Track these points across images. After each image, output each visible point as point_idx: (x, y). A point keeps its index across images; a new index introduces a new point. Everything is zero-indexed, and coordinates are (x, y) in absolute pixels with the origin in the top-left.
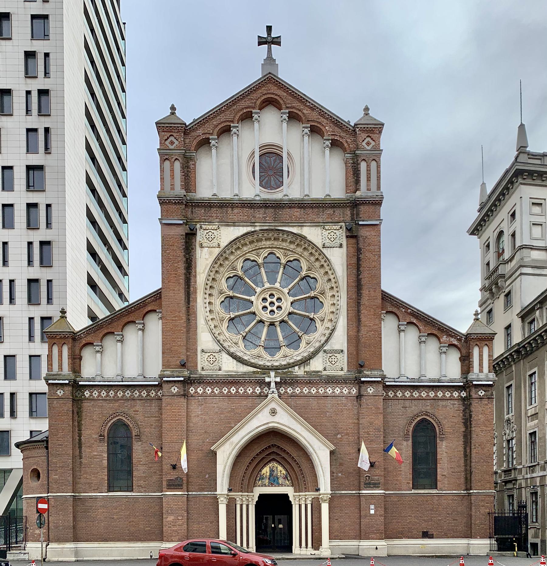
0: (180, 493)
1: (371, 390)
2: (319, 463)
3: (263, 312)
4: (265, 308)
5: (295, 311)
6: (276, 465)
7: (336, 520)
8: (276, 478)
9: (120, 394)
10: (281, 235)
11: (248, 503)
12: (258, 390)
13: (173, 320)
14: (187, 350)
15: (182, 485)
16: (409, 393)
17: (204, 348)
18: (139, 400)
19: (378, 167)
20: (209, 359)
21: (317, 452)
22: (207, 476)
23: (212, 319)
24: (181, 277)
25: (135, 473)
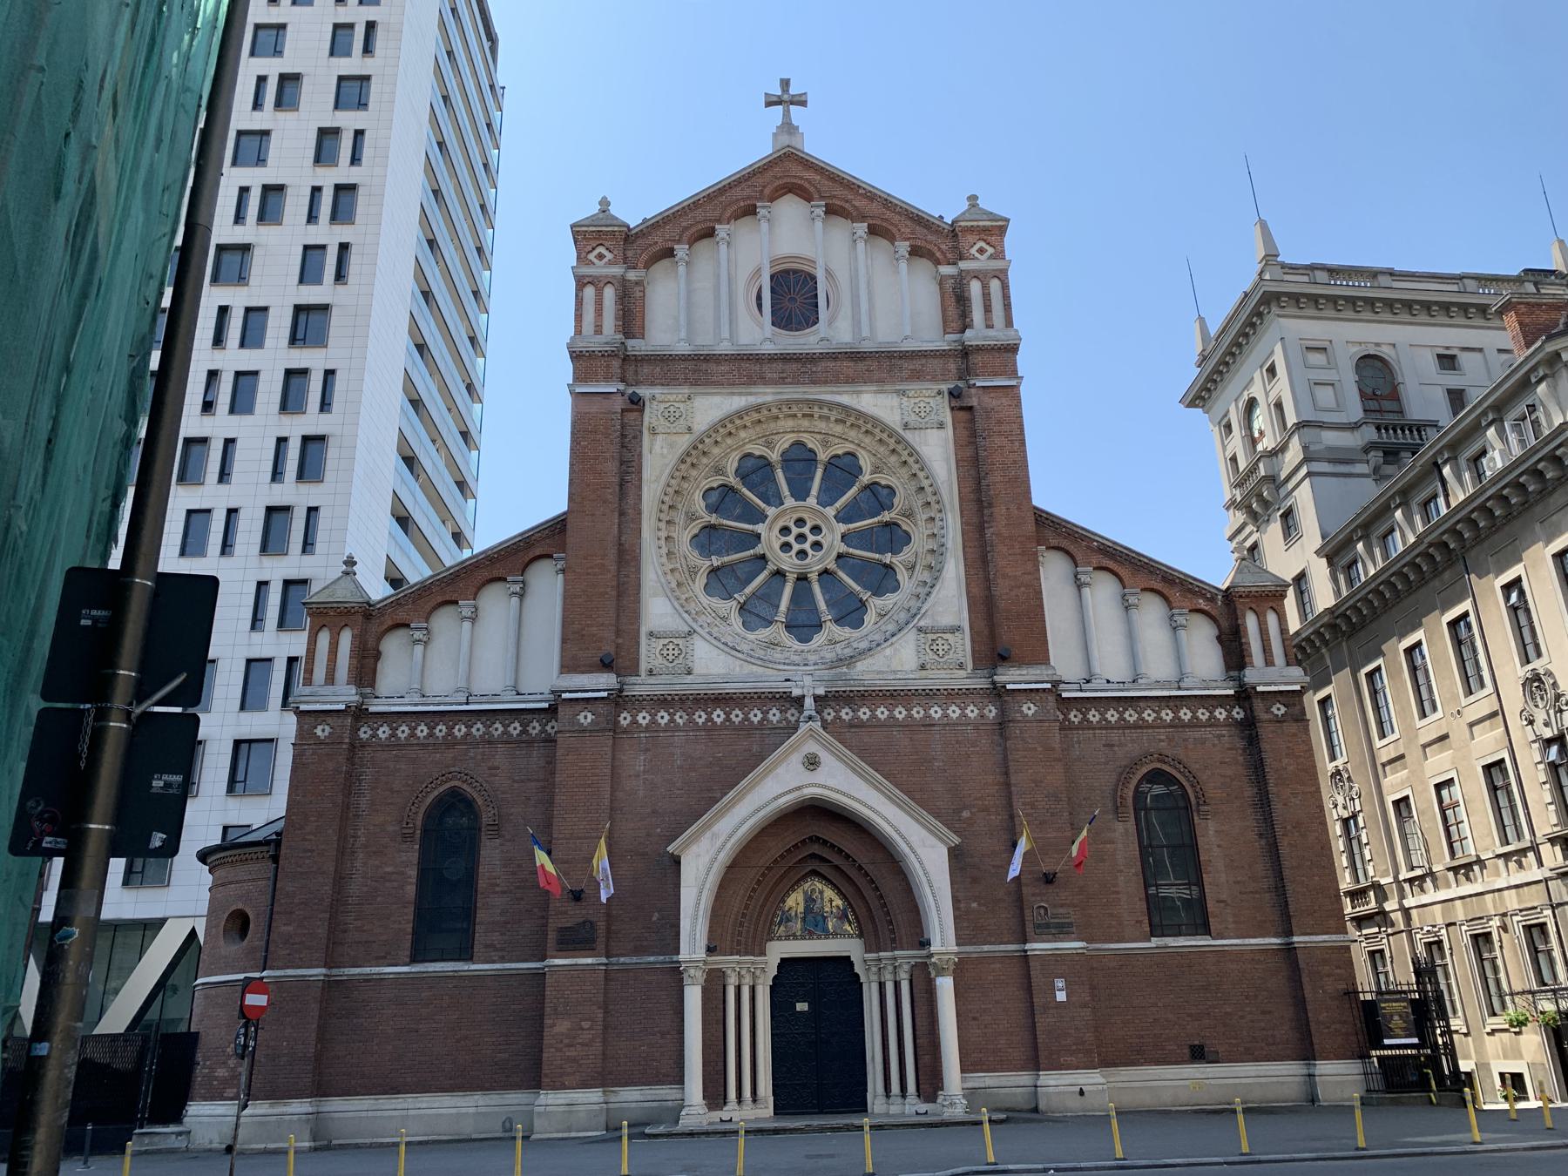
0: (589, 961)
1: (1029, 709)
2: (924, 879)
4: (786, 547)
6: (820, 886)
7: (974, 1019)
8: (819, 918)
9: (460, 730)
10: (816, 409)
11: (754, 981)
13: (588, 574)
14: (618, 633)
15: (594, 941)
16: (1115, 713)
17: (655, 629)
18: (502, 742)
19: (1005, 287)
20: (665, 652)
22: (656, 916)
23: (672, 571)
25: (481, 915)
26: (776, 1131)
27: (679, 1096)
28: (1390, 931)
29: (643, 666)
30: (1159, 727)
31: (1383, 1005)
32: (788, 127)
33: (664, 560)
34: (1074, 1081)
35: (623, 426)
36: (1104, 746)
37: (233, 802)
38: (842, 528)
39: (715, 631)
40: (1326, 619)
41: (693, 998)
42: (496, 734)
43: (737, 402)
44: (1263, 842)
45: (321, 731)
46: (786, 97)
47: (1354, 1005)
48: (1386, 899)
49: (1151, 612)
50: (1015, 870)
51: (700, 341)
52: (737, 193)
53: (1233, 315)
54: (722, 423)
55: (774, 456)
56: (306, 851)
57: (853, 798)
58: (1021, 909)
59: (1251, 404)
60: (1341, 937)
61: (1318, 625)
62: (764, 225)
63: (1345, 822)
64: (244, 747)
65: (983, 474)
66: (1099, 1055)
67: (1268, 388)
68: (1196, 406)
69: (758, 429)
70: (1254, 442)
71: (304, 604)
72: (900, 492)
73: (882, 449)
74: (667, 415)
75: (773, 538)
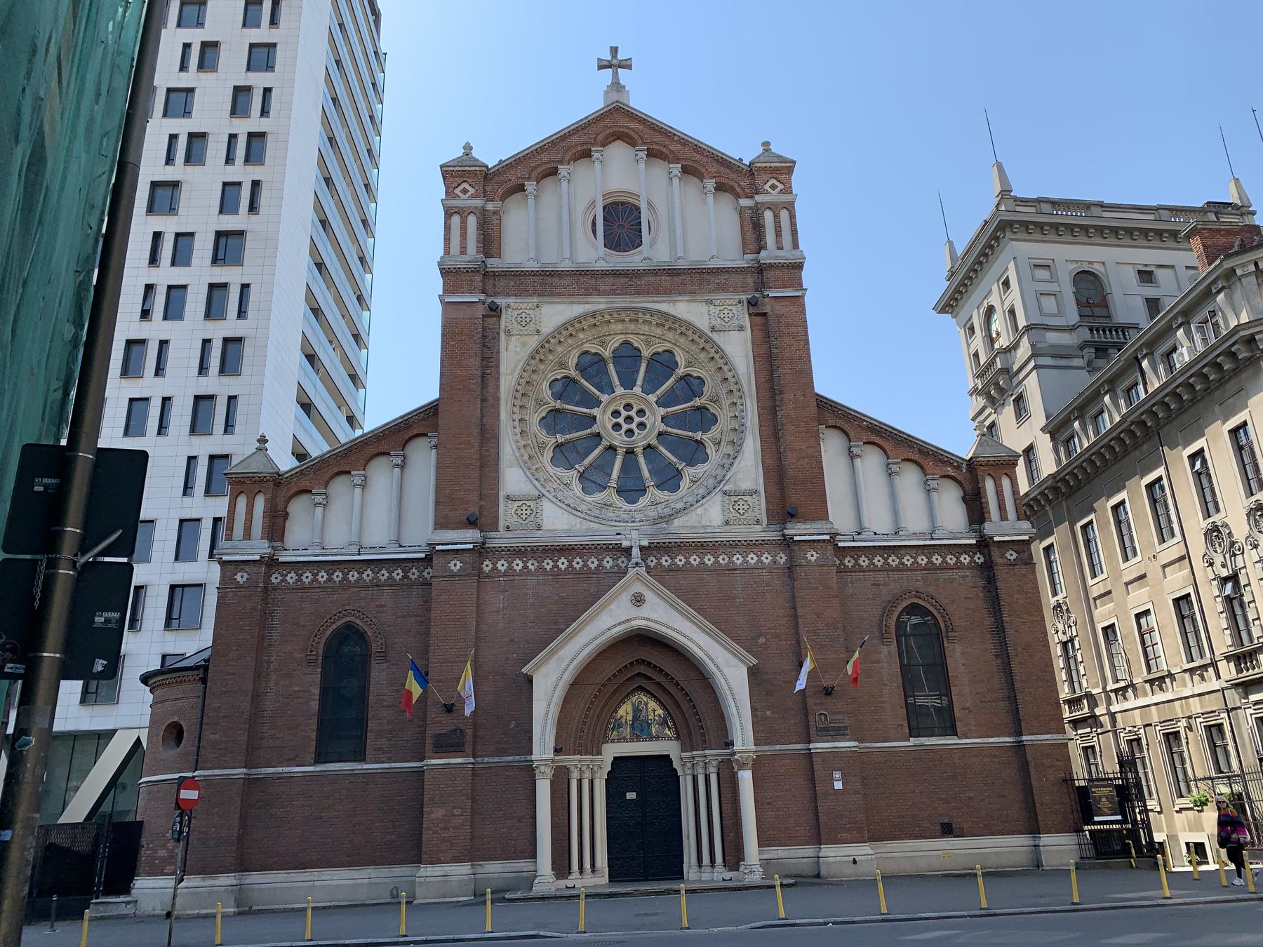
0: (460, 760)
1: (812, 556)
2: (728, 692)
3: (613, 432)
4: (617, 427)
5: (669, 429)
6: (645, 699)
7: (769, 804)
9: (353, 576)
10: (640, 315)
12: (608, 562)
13: (457, 449)
14: (481, 496)
15: (463, 745)
18: (387, 586)
19: (792, 217)
21: (724, 670)
24: (472, 382)
25: (371, 725)
26: (610, 895)
27: (532, 868)
28: (1099, 731)
29: (502, 524)
30: (916, 570)
31: (1093, 790)
32: (616, 86)
33: (518, 437)
34: (846, 853)
35: (484, 329)
36: (872, 585)
37: (169, 636)
38: (662, 411)
39: (560, 495)
40: (1049, 483)
41: (543, 790)
42: (383, 579)
43: (577, 309)
44: (999, 661)
45: (241, 577)
46: (615, 62)
47: (1071, 790)
48: (1096, 705)
49: (909, 479)
50: (801, 684)
51: (545, 260)
52: (575, 139)
53: (975, 239)
54: (565, 326)
55: (607, 354)
57: (672, 629)
58: (807, 716)
59: (990, 310)
60: (1060, 736)
61: (1043, 488)
62: (597, 165)
63: (1065, 644)
64: (178, 590)
65: (775, 368)
66: (868, 832)
67: (1004, 298)
68: (947, 312)
69: (593, 331)
70: (992, 341)
71: (225, 474)
72: (708, 382)
73: (694, 348)
74: (519, 320)
75: (607, 421)
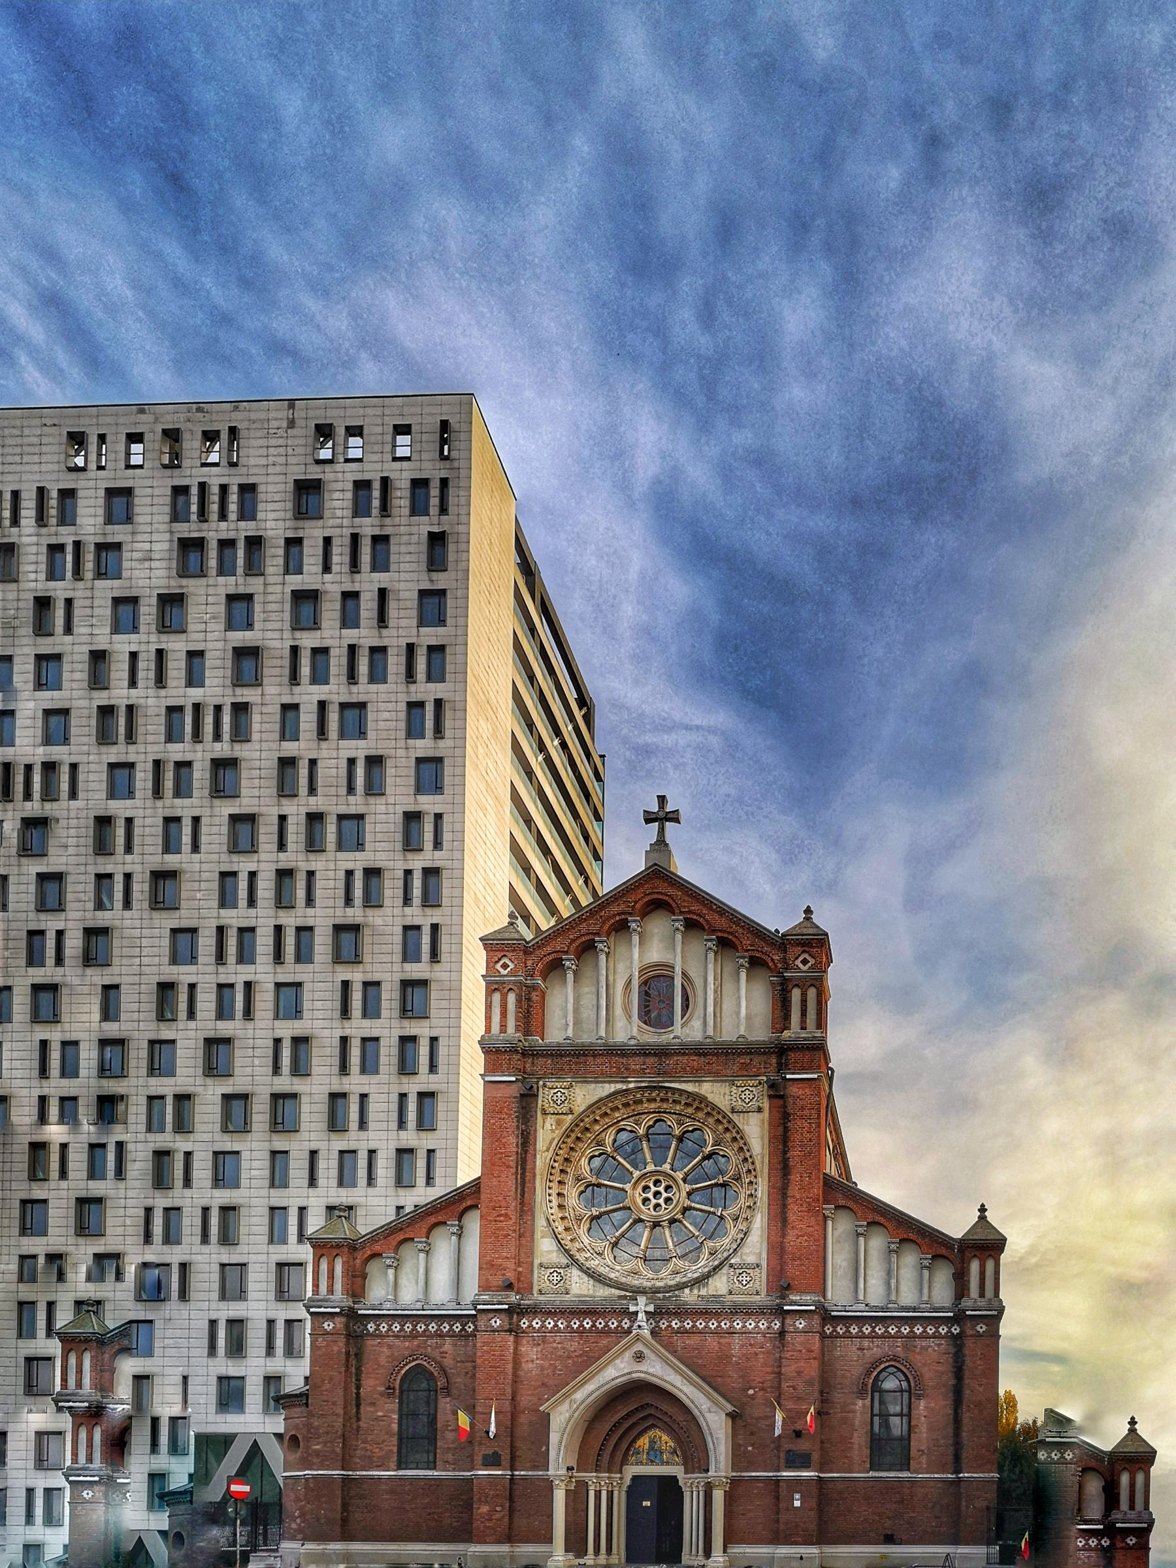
42: (445, 1330)
56: (324, 1401)
